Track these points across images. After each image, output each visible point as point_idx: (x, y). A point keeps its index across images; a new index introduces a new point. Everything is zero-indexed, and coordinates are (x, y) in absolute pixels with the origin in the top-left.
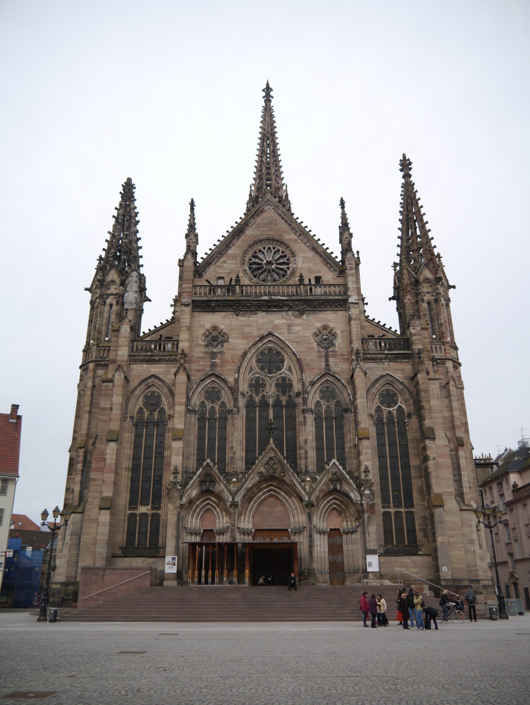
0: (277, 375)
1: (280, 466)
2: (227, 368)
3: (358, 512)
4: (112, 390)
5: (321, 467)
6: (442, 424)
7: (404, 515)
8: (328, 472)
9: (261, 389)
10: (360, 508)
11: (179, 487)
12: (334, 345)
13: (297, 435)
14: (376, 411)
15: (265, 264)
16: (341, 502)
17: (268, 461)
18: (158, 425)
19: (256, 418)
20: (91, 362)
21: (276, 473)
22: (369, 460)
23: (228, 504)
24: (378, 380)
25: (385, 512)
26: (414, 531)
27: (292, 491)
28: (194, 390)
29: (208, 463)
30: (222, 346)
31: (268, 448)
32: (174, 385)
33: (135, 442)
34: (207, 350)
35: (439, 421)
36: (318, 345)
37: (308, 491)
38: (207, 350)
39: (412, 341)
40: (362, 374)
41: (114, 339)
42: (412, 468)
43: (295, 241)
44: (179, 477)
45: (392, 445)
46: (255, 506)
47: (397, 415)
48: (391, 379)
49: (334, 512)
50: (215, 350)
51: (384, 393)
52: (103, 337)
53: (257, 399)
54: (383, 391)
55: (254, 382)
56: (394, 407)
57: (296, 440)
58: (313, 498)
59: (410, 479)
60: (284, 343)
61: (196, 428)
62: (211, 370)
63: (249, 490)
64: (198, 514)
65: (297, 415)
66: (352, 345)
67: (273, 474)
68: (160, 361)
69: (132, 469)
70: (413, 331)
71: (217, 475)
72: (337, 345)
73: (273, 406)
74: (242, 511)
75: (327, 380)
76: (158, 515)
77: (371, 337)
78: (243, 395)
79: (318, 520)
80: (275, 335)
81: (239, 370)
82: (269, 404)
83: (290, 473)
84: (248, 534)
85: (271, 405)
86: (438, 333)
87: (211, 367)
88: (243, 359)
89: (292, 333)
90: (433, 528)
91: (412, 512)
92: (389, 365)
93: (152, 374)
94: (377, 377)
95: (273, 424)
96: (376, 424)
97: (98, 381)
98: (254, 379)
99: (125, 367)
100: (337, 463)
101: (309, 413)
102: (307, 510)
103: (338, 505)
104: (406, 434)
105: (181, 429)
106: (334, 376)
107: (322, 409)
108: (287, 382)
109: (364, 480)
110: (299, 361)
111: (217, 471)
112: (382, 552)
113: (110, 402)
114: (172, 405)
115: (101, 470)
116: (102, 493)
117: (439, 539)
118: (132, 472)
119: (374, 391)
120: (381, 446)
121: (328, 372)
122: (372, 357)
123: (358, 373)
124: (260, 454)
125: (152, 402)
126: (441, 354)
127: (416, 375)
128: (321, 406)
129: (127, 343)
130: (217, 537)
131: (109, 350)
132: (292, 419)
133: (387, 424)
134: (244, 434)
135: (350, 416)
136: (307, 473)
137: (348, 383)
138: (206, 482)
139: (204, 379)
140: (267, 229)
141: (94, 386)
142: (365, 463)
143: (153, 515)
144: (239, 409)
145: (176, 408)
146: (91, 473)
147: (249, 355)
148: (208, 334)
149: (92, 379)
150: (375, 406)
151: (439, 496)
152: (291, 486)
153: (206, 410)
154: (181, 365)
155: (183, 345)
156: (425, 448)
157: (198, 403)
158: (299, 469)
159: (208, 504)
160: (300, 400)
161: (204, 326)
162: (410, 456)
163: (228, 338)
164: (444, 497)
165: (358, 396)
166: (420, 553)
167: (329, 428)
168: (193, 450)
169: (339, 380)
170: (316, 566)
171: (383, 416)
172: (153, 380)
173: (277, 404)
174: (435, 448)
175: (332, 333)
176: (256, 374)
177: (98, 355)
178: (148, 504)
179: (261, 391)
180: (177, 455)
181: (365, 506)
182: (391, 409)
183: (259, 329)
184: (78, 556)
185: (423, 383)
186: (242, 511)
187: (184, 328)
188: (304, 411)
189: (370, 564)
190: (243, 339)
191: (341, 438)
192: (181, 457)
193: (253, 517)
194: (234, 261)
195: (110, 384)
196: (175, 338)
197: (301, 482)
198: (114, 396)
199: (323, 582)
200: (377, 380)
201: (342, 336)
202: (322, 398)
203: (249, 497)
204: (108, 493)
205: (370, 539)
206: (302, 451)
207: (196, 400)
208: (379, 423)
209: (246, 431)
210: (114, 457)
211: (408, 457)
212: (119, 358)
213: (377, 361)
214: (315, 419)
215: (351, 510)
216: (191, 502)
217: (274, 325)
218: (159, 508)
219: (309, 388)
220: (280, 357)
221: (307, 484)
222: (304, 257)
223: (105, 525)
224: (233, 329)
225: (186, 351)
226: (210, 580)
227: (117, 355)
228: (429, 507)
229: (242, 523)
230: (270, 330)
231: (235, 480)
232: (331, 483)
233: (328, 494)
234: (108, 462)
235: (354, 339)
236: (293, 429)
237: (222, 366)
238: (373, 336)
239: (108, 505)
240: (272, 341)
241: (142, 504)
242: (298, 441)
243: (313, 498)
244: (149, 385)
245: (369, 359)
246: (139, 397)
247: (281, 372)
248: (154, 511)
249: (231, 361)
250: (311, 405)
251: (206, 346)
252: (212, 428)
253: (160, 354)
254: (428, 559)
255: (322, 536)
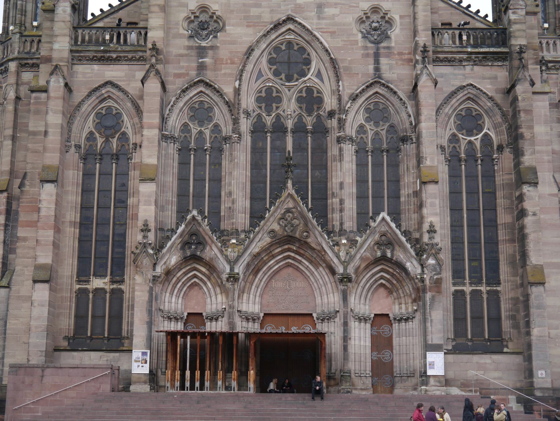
0: (300, 84)
1: (302, 222)
2: (223, 72)
3: (417, 290)
4: (46, 104)
5: (363, 225)
6: (549, 162)
7: (485, 296)
8: (373, 232)
9: (274, 105)
10: (420, 284)
11: (151, 252)
12: (388, 37)
13: (329, 176)
14: (450, 141)
16: (392, 275)
17: (284, 214)
18: (118, 159)
19: (266, 148)
20: (12, 60)
21: (295, 233)
22: (436, 214)
23: (224, 276)
24: (455, 93)
25: (456, 291)
26: (499, 319)
27: (319, 259)
28: (172, 106)
29: (194, 217)
30: (215, 37)
31: (285, 194)
32: (141, 97)
33: (83, 183)
34: (191, 43)
35: (546, 158)
36: (364, 37)
37: (343, 259)
38: (191, 43)
39: (510, 32)
40: (430, 84)
41: (47, 24)
42: (500, 227)
44: (151, 236)
45: (472, 192)
46: (264, 280)
47: (481, 147)
48: (474, 91)
49: (382, 290)
50: (204, 44)
51: (463, 113)
52: (28, 20)
53: (269, 120)
54: (461, 110)
55: (263, 94)
56: (477, 135)
57: (326, 183)
58: (351, 270)
59: (497, 244)
60: (312, 33)
61: (176, 164)
62: (198, 75)
63: (255, 256)
64: (180, 290)
65: (329, 145)
66: (417, 39)
67: (290, 234)
68: (119, 60)
69: (81, 224)
70: (513, 17)
71: (207, 235)
72: (393, 37)
73: (293, 132)
74: (244, 287)
75: (377, 93)
76: (121, 292)
77: (447, 25)
78: (248, 114)
79: (357, 301)
80: (296, 21)
81: (241, 76)
82: (286, 128)
83: (317, 233)
84: (254, 320)
85: (289, 129)
86: (552, 20)
87: (198, 70)
88: (248, 58)
89: (323, 18)
90: (528, 315)
91: (497, 292)
92: (472, 70)
93: (108, 79)
94: (453, 89)
95: (293, 160)
96: (449, 161)
97: (24, 90)
98: (264, 89)
99: (65, 69)
100: (388, 219)
101: (347, 142)
102: (341, 287)
103: (388, 280)
104: (494, 177)
105: (153, 165)
106: (388, 87)
107: (367, 137)
108: (315, 94)
109: (427, 245)
110: (333, 62)
111: (208, 228)
112: (450, 348)
113: (44, 123)
114: (139, 128)
115: (33, 224)
116: (36, 258)
117: (535, 332)
118: (80, 228)
119: (447, 109)
120: (454, 193)
121: (377, 80)
122: (446, 58)
123: (424, 83)
124: (272, 204)
125: (109, 123)
126: (555, 53)
127: (513, 86)
128: (365, 132)
129: (67, 31)
130: (208, 324)
131: (40, 41)
132: (321, 151)
133: (466, 160)
134: (249, 174)
135: (409, 148)
136: (342, 232)
137: (409, 97)
138: (192, 244)
139: (187, 88)
141: (18, 98)
142: (429, 220)
143: (113, 291)
144: (240, 135)
145: (146, 132)
146: (19, 228)
147: (257, 53)
148: (193, 18)
149: (15, 86)
150: (448, 134)
151: (540, 269)
152: (319, 251)
153: (191, 137)
154: (152, 66)
155: (155, 35)
156: (521, 198)
157: (178, 126)
158: (330, 227)
159: (195, 276)
160: (334, 123)
161: (186, 5)
162: (499, 210)
163: (224, 25)
164: (546, 271)
165: (423, 118)
166: (505, 350)
167: (377, 165)
168: (171, 196)
169: (395, 93)
170: (352, 366)
171: (460, 149)
172: (108, 89)
173: (300, 129)
174: (537, 198)
175: (387, 19)
176: (269, 82)
177: (21, 49)
178: (105, 276)
179: (274, 108)
180: (147, 203)
181: (427, 282)
182: (472, 139)
183: (272, 11)
184: (4, 350)
185: (524, 100)
186: (244, 287)
187: (156, 9)
188: (339, 140)
189: (432, 365)
190: (248, 26)
191: (395, 182)
192: (153, 207)
193: (261, 296)
195: (44, 95)
196: (141, 24)
197: (334, 245)
198: (50, 113)
199: (362, 389)
200: (453, 94)
201: (401, 24)
202: (368, 120)
203: (254, 268)
204: (45, 258)
205: (433, 329)
206: (336, 201)
207: (175, 122)
208: (453, 160)
209: (252, 169)
210: (53, 206)
211: (495, 210)
212: (55, 55)
213: (454, 63)
214: (357, 152)
215: (406, 288)
216: (168, 273)
217: (296, 5)
218: (122, 281)
219: (349, 105)
220: (305, 56)
221: (343, 248)
223: (43, 306)
224: (232, 11)
225: (159, 45)
226: (197, 384)
227: (52, 49)
228: (522, 285)
229: (244, 304)
230: (290, 12)
231: (234, 241)
232: (378, 248)
233: (373, 264)
234: (43, 213)
235: (420, 28)
236: (322, 166)
237: (215, 70)
238: (450, 24)
239: (45, 276)
240: (293, 31)
241: (95, 275)
242: (329, 185)
243: (351, 270)
244: (103, 97)
245: (441, 61)
246: (88, 115)
247: (306, 79)
248: (115, 286)
249: (229, 61)
250: (350, 130)
251: (191, 37)
252: (200, 164)
253: (119, 49)
254: (518, 359)
255: (362, 324)
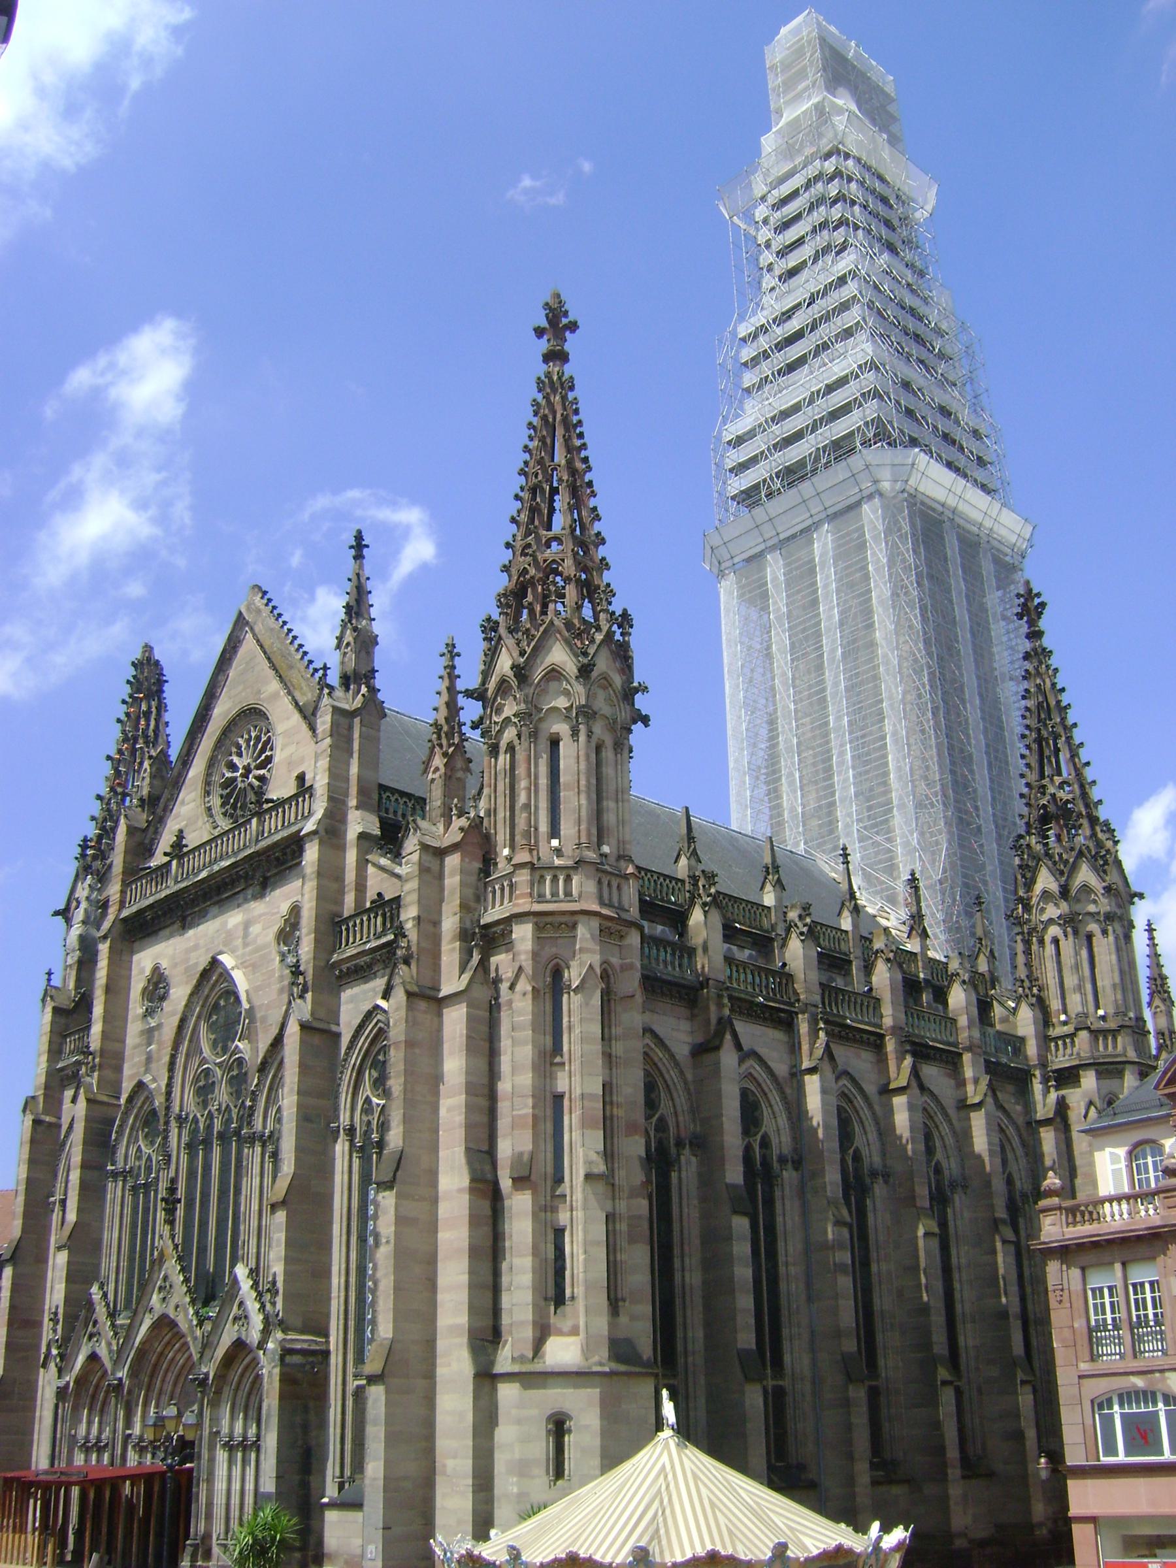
15: (242, 775)
43: (275, 696)
140: (241, 687)
185: (395, 1024)
194: (193, 795)
222: (285, 733)
